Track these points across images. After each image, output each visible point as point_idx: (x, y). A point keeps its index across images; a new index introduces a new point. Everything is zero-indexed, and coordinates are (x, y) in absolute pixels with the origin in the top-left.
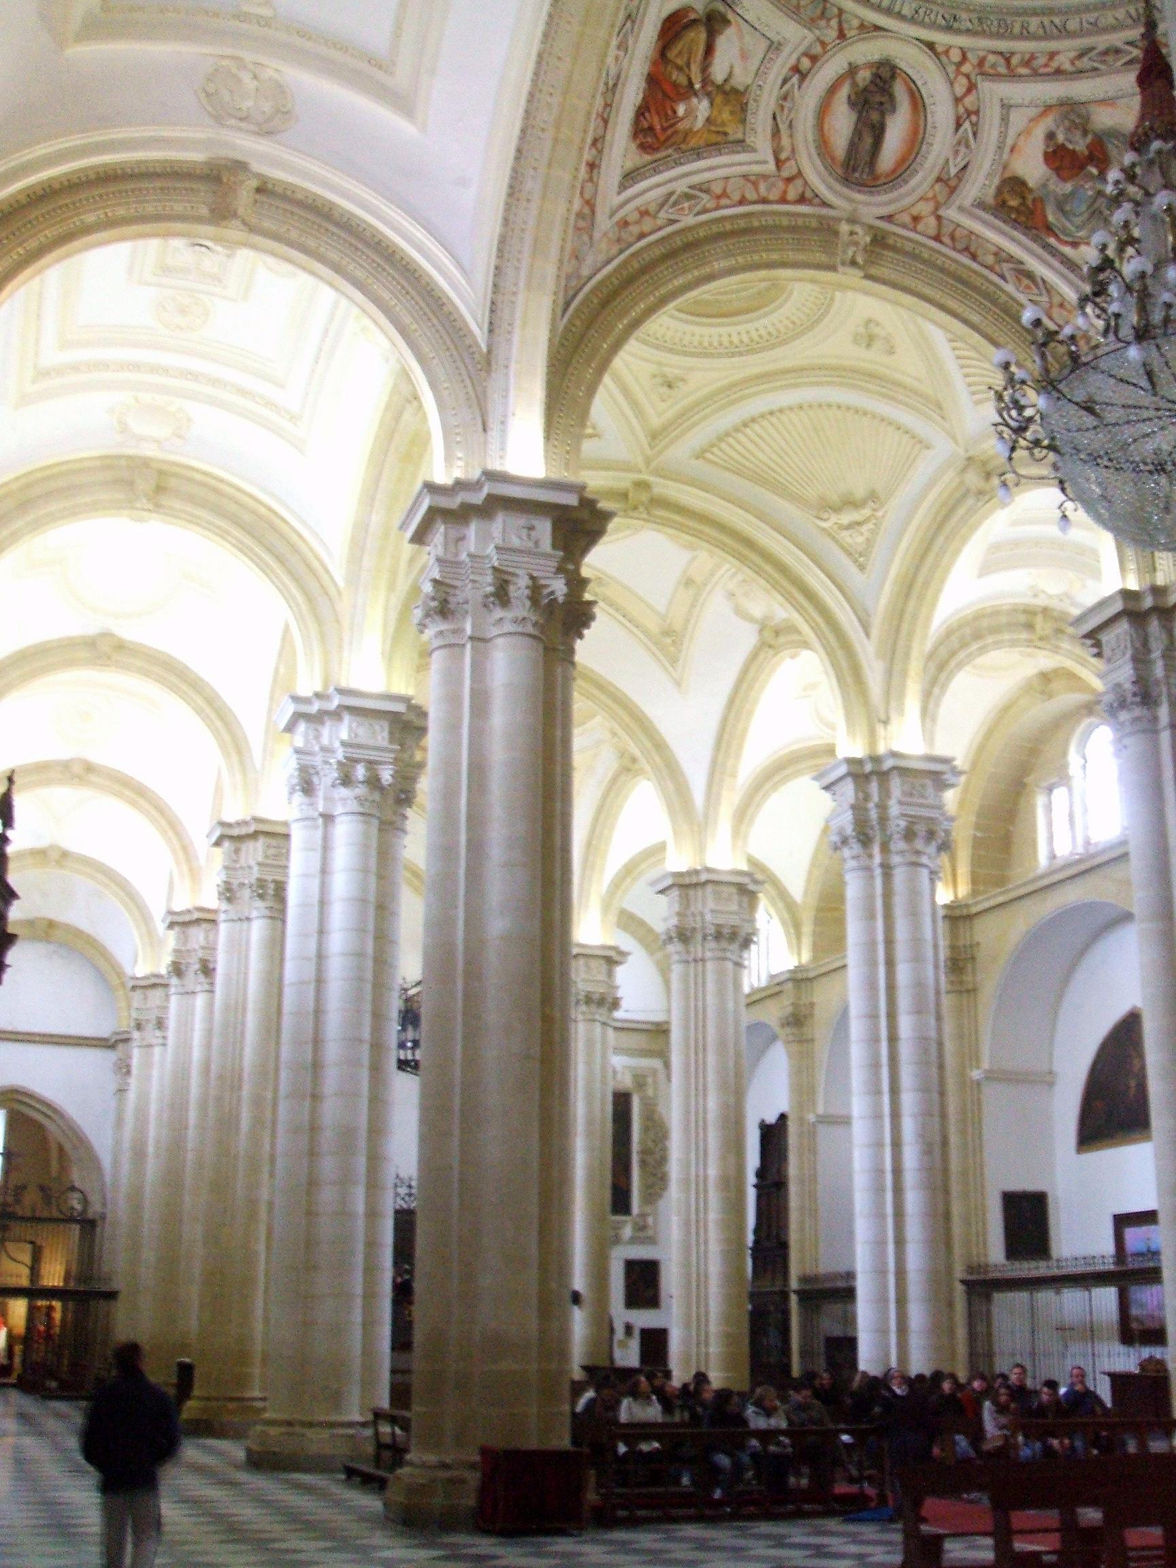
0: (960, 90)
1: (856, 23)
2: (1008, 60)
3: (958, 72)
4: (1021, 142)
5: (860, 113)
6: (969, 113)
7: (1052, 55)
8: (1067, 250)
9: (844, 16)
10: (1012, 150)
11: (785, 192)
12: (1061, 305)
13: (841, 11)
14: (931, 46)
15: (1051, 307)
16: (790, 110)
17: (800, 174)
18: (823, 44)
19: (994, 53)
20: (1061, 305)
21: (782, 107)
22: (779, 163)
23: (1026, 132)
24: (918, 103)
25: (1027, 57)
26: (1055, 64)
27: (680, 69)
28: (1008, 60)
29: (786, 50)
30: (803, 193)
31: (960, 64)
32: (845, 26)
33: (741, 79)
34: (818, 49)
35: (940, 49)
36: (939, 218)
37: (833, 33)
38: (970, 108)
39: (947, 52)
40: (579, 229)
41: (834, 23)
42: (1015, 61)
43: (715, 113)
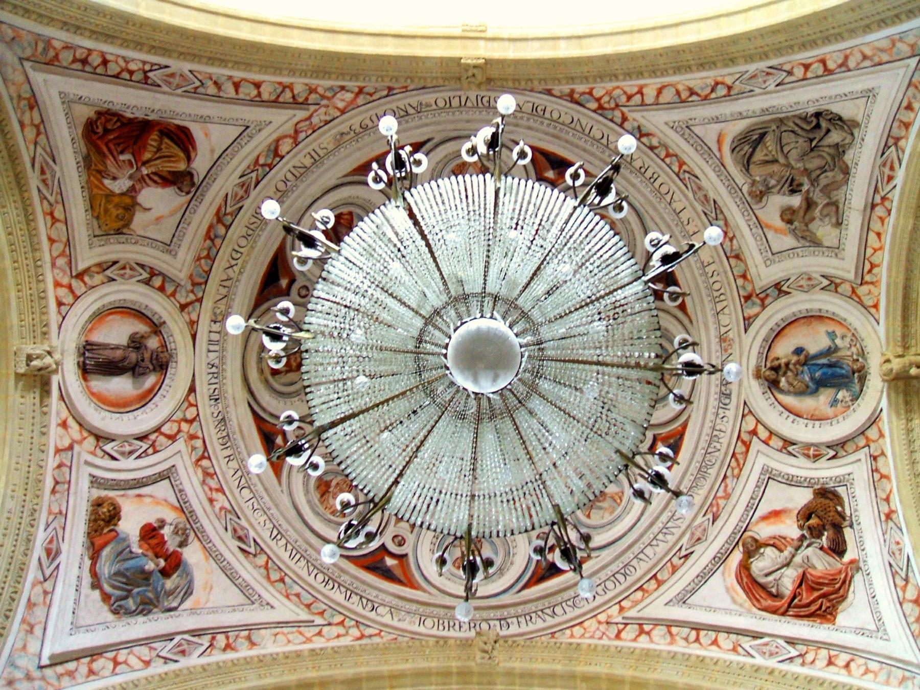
0: (165, 429)
1: (194, 317)
2: (203, 457)
3: (179, 422)
4: (148, 500)
5: (128, 347)
6: (153, 445)
7: (221, 490)
8: (87, 579)
9: (197, 304)
10: (139, 496)
11: (62, 286)
12: (46, 593)
13: (200, 300)
14: (192, 389)
15: (41, 583)
16: (122, 276)
17: (77, 298)
18: (173, 294)
19: (204, 442)
20: (46, 593)
21: (124, 268)
22: (80, 276)
23: (157, 501)
24: (146, 398)
25: (211, 471)
26: (215, 495)
27: (159, 149)
28: (203, 457)
29: (167, 257)
30: (64, 304)
31: (186, 421)
32: (190, 308)
33: (139, 220)
34: (170, 289)
35: (191, 398)
36: (71, 448)
37: (183, 301)
38: (157, 444)
39: (191, 405)
40: (36, 44)
41: (192, 297)
42: (205, 463)
43: (116, 200)
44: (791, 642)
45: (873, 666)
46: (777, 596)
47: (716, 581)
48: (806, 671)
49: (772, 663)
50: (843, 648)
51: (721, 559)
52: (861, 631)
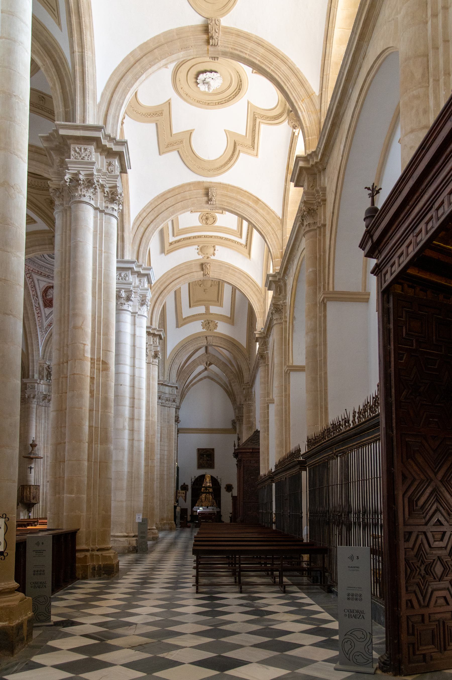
44: (39, 304)
45: (40, 321)
46: (46, 296)
47: (45, 283)
48: (35, 310)
49: (34, 304)
50: (41, 314)
51: (50, 283)
52: (45, 314)
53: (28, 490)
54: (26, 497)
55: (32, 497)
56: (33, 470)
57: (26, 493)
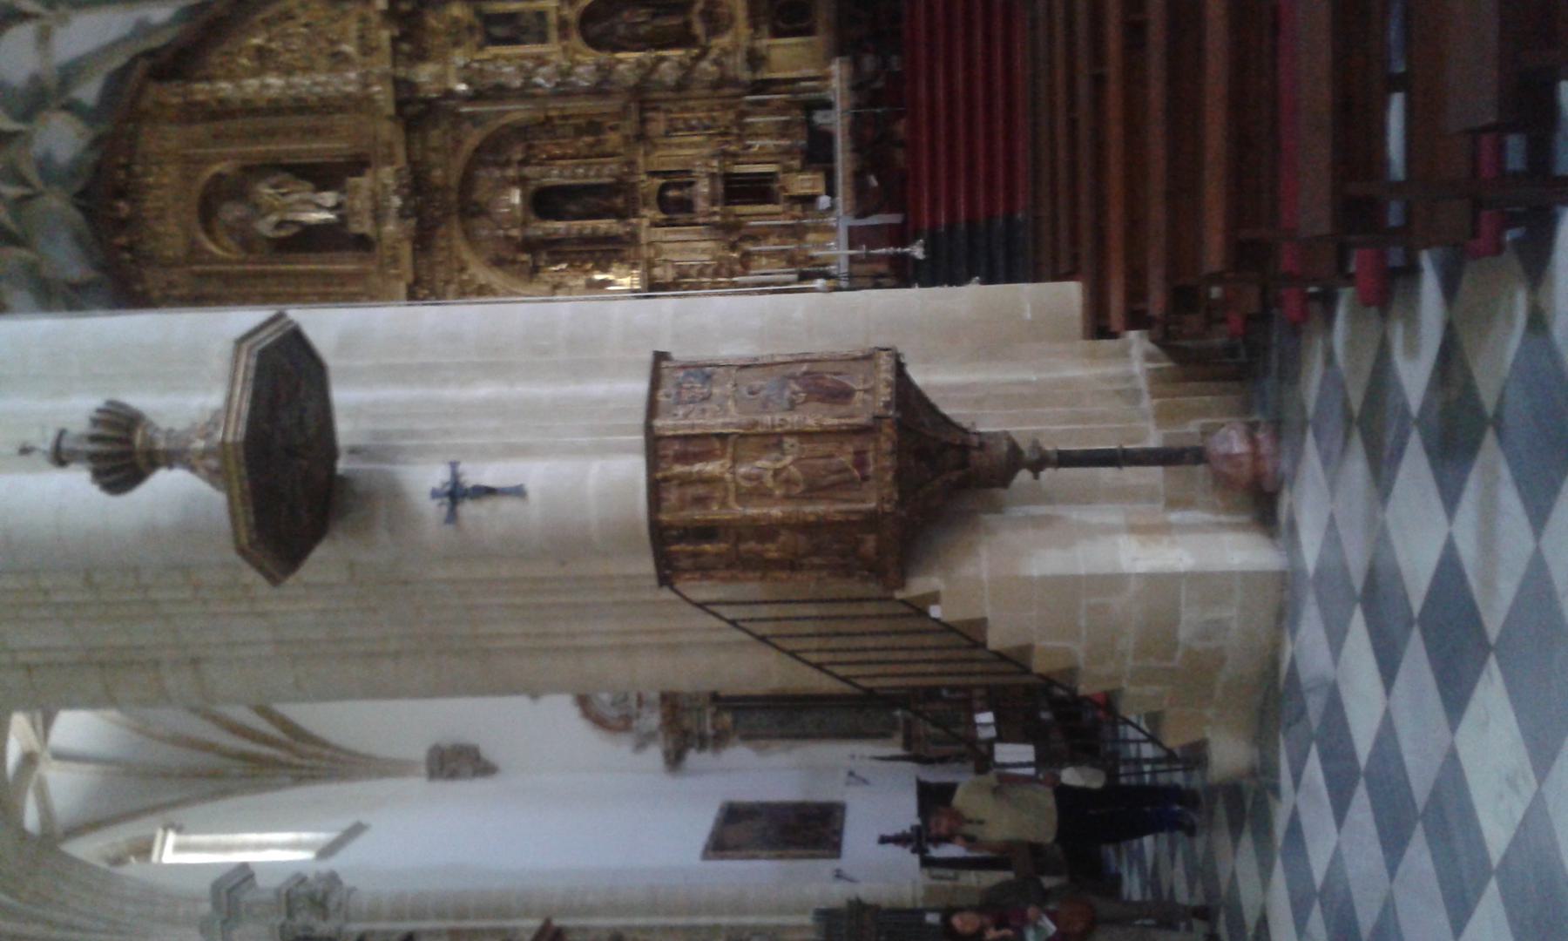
53: (711, 468)
54: (814, 490)
55: (815, 417)
56: (479, 473)
57: (758, 491)
